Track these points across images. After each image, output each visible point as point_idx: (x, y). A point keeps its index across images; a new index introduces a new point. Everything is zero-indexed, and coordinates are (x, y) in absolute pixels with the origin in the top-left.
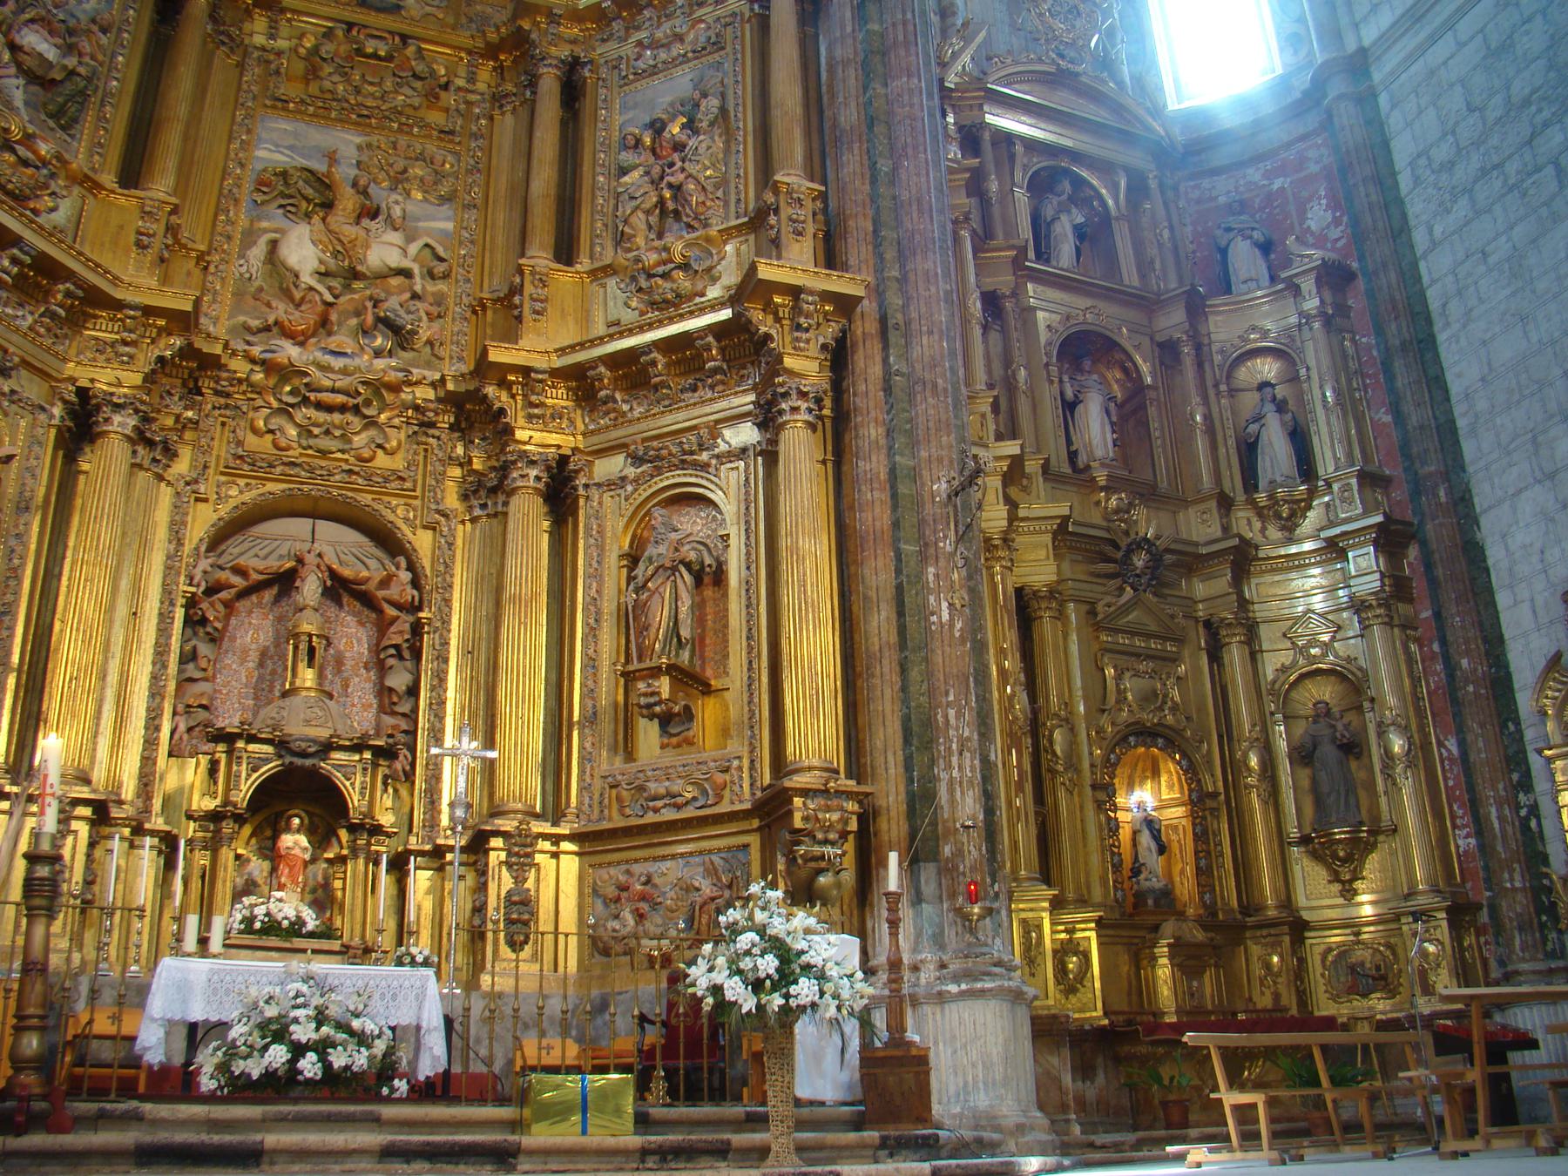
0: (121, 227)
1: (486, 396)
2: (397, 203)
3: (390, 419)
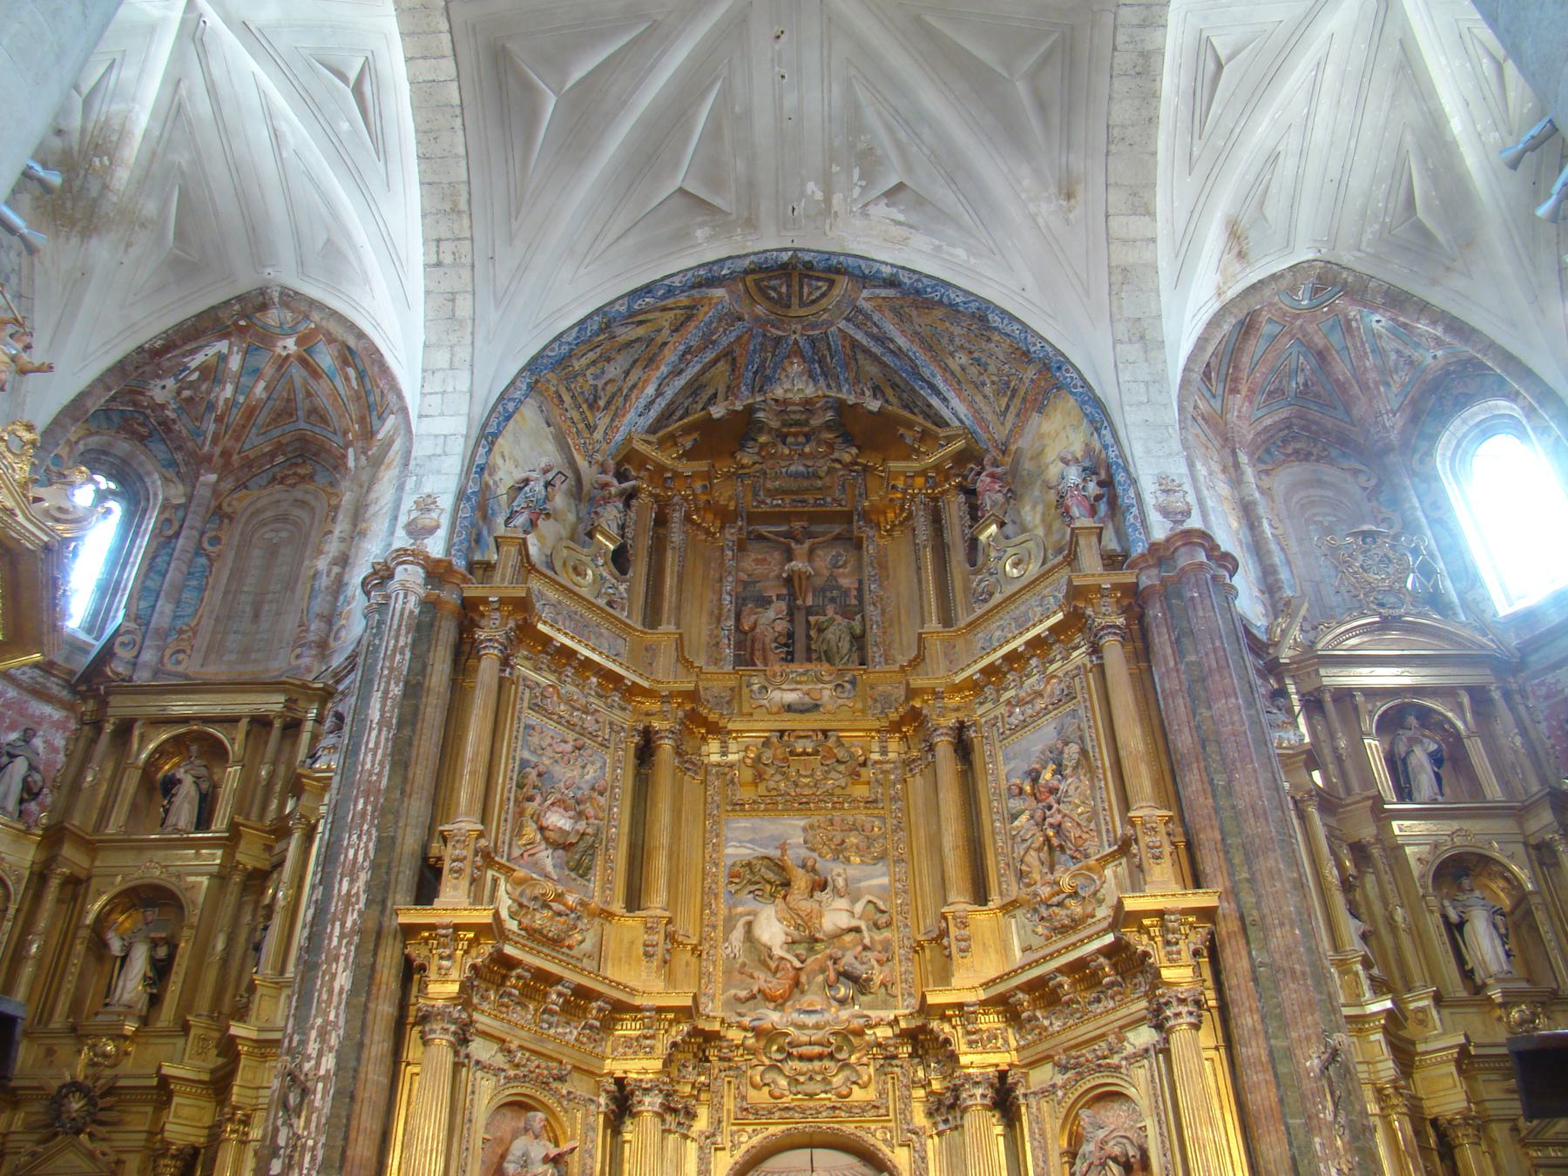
0: (632, 943)
1: (932, 1030)
2: (839, 875)
3: (859, 1059)
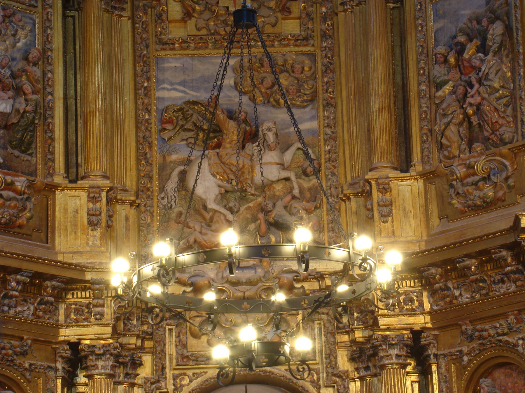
2: (269, 130)
